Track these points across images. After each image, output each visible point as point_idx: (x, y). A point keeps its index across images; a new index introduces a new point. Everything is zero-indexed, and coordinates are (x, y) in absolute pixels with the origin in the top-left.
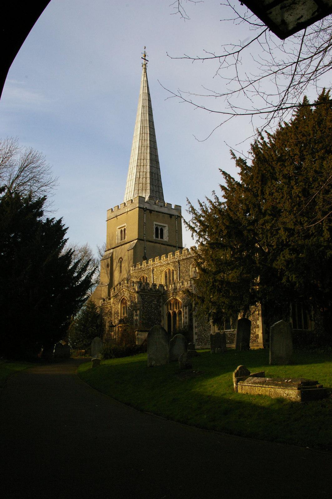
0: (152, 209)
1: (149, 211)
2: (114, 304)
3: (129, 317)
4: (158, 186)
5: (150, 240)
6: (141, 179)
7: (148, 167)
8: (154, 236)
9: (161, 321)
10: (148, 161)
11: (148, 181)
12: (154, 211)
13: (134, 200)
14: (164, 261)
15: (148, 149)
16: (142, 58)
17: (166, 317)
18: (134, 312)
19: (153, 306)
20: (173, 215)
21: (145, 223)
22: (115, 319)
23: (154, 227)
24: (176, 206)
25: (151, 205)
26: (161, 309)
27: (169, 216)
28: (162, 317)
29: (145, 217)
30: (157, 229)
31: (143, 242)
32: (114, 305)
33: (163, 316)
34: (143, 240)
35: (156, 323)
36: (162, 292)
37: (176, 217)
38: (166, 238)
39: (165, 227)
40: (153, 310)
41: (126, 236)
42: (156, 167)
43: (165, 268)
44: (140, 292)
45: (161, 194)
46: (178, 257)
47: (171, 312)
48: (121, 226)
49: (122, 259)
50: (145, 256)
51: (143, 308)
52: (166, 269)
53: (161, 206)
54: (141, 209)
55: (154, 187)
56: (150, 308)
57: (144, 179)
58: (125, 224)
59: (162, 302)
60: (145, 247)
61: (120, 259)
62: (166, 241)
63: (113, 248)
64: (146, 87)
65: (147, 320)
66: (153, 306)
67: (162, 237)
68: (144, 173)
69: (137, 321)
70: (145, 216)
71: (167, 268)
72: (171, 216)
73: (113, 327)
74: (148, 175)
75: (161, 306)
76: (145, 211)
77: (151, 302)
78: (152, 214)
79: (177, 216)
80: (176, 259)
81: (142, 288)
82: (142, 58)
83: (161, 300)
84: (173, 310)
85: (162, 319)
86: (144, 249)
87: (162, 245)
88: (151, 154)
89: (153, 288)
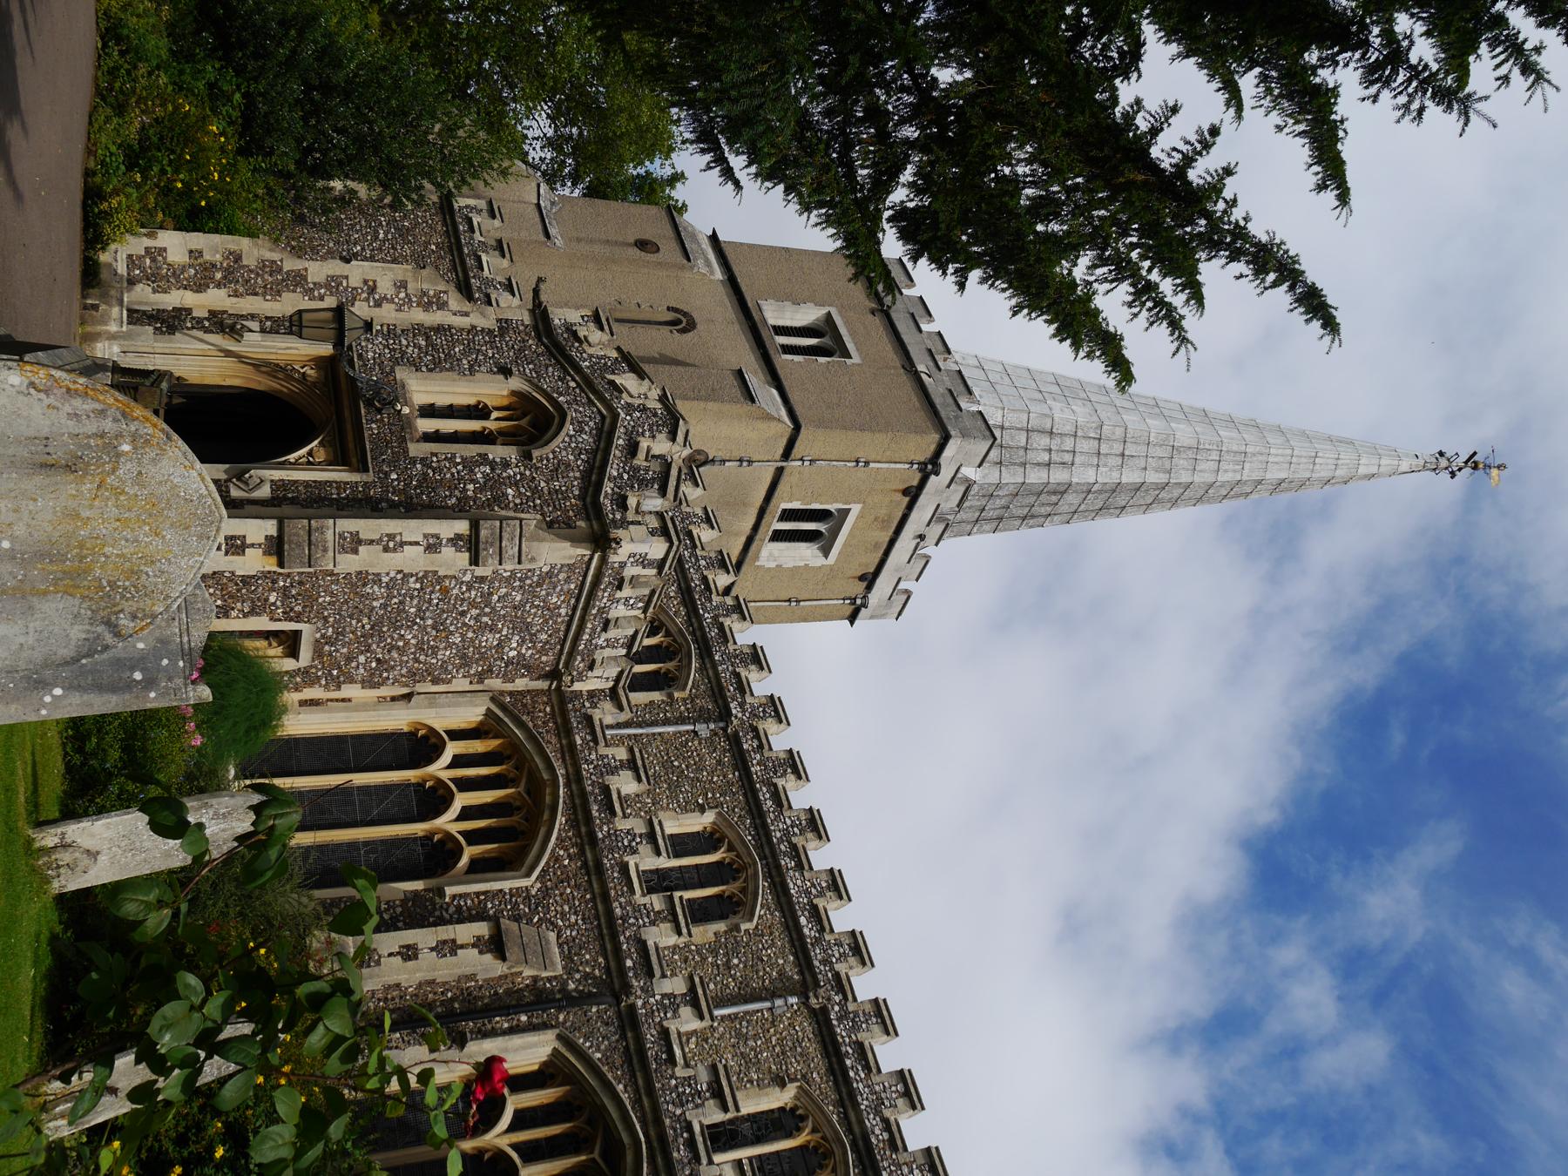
0: (922, 499)
1: (915, 483)
2: (502, 335)
3: (413, 461)
4: (1000, 519)
5: (782, 488)
6: (1044, 441)
7: (1089, 476)
8: (796, 505)
9: (369, 683)
10: (1114, 477)
11: (1036, 477)
12: (910, 507)
13: (973, 414)
14: (715, 618)
15: (1162, 475)
16: (1475, 453)
17: (397, 720)
18: (462, 527)
19: (491, 639)
20: (869, 588)
21: (867, 463)
22: (391, 332)
23: (832, 507)
24: (908, 594)
25: (938, 492)
26: (461, 684)
27: (872, 570)
28: (405, 691)
29: (893, 466)
30: (822, 515)
31: (781, 451)
32: (490, 332)
33: (408, 697)
34: (786, 455)
35: (362, 659)
36: (577, 686)
37: (859, 602)
38: (772, 555)
39: (826, 552)
40: (462, 635)
41: (798, 358)
42: (1083, 507)
43: (678, 621)
44: (603, 560)
45: (969, 527)
46: (754, 715)
47: (439, 769)
48: (843, 331)
49: (683, 331)
50: (705, 463)
51: (482, 579)
52: (673, 630)
53: (922, 537)
54: (933, 447)
55: (1003, 502)
56: (477, 619)
57: (1045, 457)
58: (856, 359)
59: (509, 687)
60: (750, 462)
61: (685, 314)
62: (757, 558)
63: (732, 281)
64: (1374, 470)
65: (384, 606)
66: (491, 639)
67: (778, 536)
68: (1068, 458)
69: (386, 549)
70: (898, 466)
71: (680, 640)
72: (870, 580)
73: (331, 333)
74: (1058, 476)
75: (481, 681)
76: (923, 466)
77: (522, 627)
78: (899, 496)
79: (864, 605)
80: (742, 705)
81: (630, 571)
82: (1475, 453)
83: (521, 684)
84: (466, 785)
85: (386, 691)
86: (741, 460)
87: (743, 539)
88: (1138, 488)
89: (612, 633)
